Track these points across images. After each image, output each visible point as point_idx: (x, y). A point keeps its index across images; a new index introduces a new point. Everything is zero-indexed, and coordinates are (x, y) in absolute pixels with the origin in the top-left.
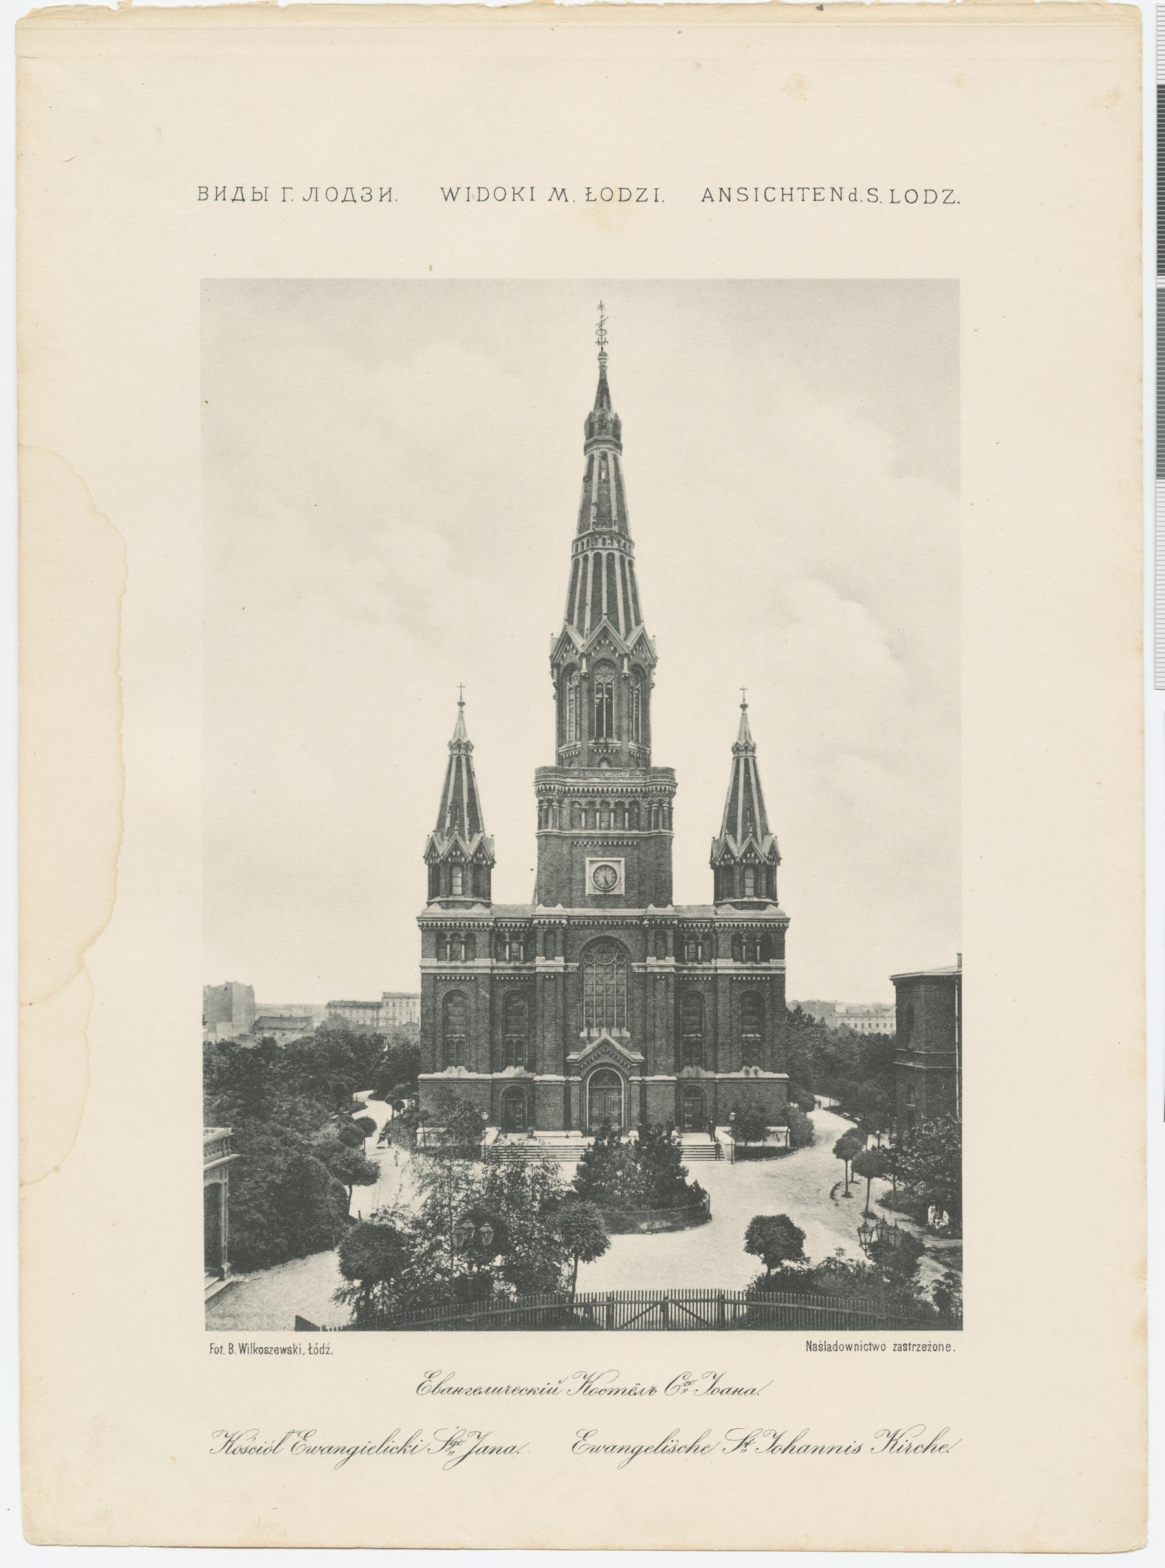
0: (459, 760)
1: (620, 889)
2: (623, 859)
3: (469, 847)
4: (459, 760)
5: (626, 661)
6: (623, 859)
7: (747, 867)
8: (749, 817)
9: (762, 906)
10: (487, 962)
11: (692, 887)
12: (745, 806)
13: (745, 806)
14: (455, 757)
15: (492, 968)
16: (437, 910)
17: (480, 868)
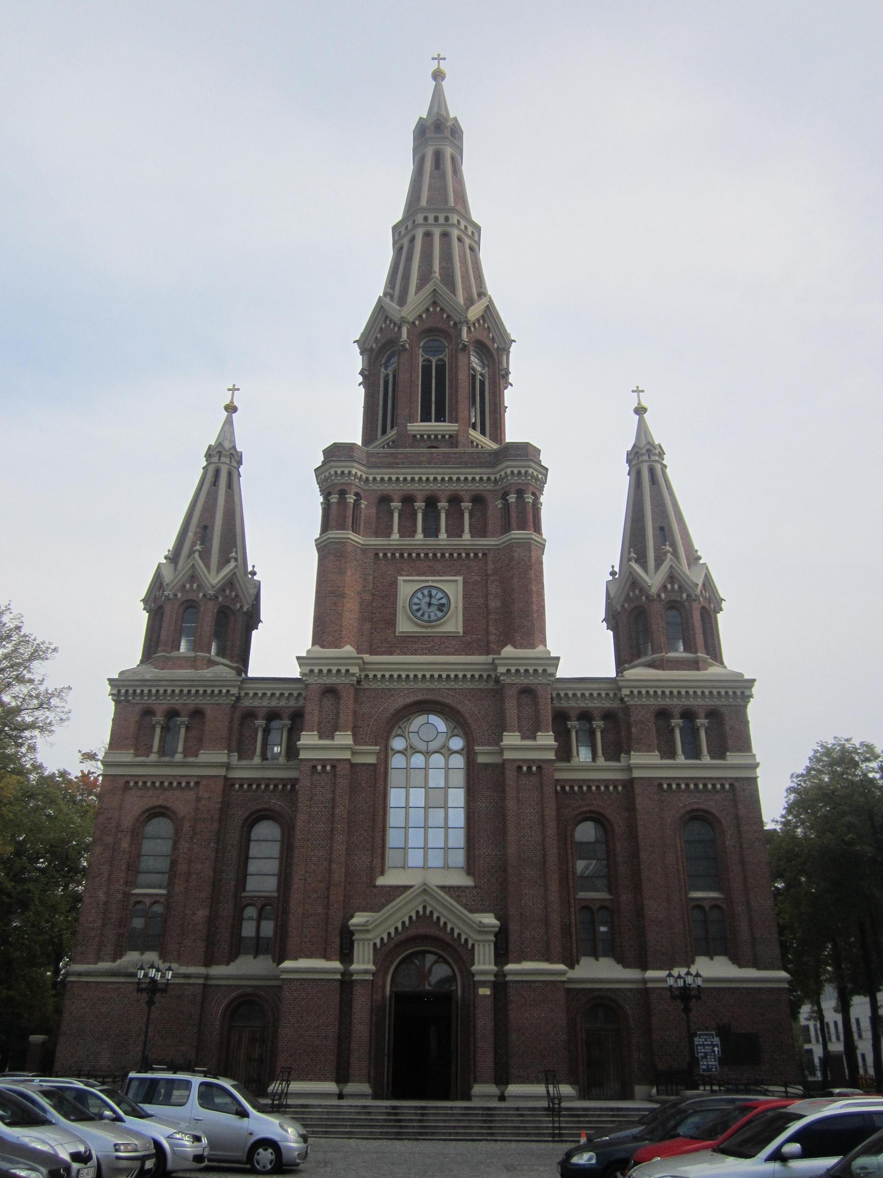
0: (217, 472)
1: (454, 624)
2: (460, 579)
3: (214, 579)
4: (217, 472)
5: (465, 329)
6: (460, 579)
7: (663, 608)
8: (664, 533)
9: (695, 665)
10: (221, 757)
11: (578, 642)
12: (651, 518)
13: (651, 518)
14: (211, 469)
15: (228, 766)
16: (151, 673)
17: (233, 616)
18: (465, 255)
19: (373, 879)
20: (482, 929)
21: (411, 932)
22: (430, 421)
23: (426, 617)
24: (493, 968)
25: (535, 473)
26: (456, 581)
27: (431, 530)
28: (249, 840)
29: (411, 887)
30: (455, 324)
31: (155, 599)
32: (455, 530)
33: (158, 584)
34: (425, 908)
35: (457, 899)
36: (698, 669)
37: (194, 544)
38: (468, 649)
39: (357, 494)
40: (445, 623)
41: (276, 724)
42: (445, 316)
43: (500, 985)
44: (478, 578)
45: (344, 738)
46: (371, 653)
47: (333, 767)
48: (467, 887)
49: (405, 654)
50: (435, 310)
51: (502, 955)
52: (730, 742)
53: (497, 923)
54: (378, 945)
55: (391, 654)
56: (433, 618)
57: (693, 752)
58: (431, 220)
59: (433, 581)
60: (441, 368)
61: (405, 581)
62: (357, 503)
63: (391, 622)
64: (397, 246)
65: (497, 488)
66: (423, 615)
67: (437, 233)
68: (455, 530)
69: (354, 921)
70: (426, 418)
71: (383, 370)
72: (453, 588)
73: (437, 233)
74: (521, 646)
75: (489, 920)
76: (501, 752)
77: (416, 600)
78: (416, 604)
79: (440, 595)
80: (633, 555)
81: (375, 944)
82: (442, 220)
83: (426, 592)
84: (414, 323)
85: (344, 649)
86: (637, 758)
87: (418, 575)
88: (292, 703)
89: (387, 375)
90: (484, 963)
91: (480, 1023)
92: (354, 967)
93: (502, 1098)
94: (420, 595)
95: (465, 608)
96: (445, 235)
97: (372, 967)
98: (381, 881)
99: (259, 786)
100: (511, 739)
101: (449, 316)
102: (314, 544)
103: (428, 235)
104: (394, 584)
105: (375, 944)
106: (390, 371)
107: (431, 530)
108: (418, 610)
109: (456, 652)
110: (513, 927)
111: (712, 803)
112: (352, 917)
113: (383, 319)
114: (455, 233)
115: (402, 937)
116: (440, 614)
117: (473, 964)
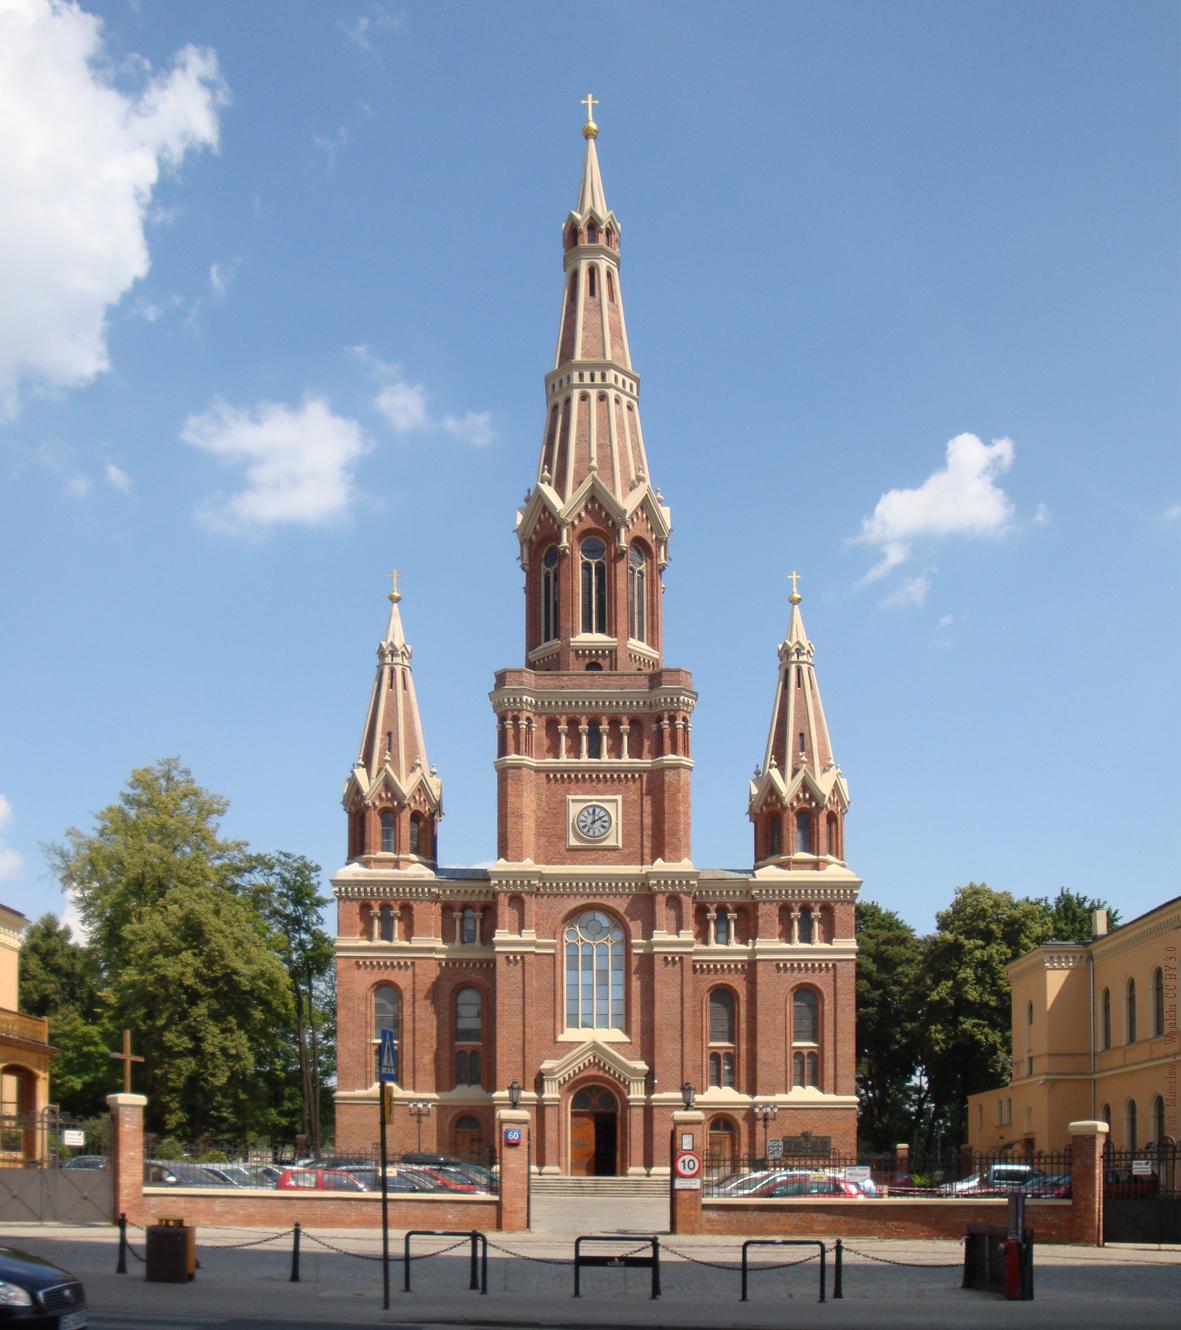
1: (614, 839)
2: (619, 798)
6: (619, 798)
9: (816, 865)
18: (622, 414)
19: (555, 1037)
20: (635, 1072)
21: (585, 1074)
22: (591, 631)
23: (591, 833)
24: (643, 1096)
25: (686, 699)
26: (616, 801)
27: (595, 752)
28: (456, 1005)
29: (581, 1043)
30: (613, 523)
31: (354, 803)
32: (616, 751)
33: (354, 792)
34: (594, 1057)
35: (618, 1050)
36: (818, 870)
37: (382, 754)
38: (626, 860)
39: (528, 719)
40: (605, 839)
41: (469, 913)
42: (603, 514)
43: (648, 1110)
44: (635, 797)
45: (529, 935)
46: (548, 862)
47: (522, 958)
48: (625, 1043)
49: (575, 864)
50: (593, 507)
51: (650, 1088)
52: (837, 931)
53: (647, 1068)
54: (562, 1082)
55: (563, 864)
56: (597, 834)
57: (806, 937)
58: (587, 380)
59: (597, 800)
60: (600, 569)
61: (573, 801)
62: (529, 727)
63: (564, 838)
64: (551, 404)
65: (653, 711)
66: (588, 831)
67: (593, 394)
68: (616, 751)
69: (543, 1066)
70: (588, 628)
71: (543, 565)
72: (613, 805)
73: (593, 394)
74: (670, 860)
75: (642, 1066)
76: (652, 945)
77: (582, 818)
78: (583, 821)
79: (602, 813)
80: (773, 762)
81: (559, 1082)
82: (598, 380)
83: (591, 811)
84: (573, 523)
85: (524, 862)
86: (761, 944)
87: (584, 794)
88: (482, 898)
89: (549, 572)
90: (637, 1093)
91: (634, 1132)
92: (545, 1096)
93: (648, 1175)
94: (585, 813)
95: (624, 825)
96: (602, 397)
97: (558, 1096)
98: (561, 1038)
99: (461, 964)
100: (659, 936)
101: (607, 514)
102: (493, 766)
103: (584, 397)
104: (564, 803)
105: (559, 1082)
106: (551, 570)
107: (595, 752)
108: (584, 827)
109: (617, 863)
110: (658, 1070)
111: (817, 978)
112: (542, 1063)
113: (541, 509)
114: (612, 394)
115: (577, 1077)
116: (602, 830)
117: (629, 1094)
